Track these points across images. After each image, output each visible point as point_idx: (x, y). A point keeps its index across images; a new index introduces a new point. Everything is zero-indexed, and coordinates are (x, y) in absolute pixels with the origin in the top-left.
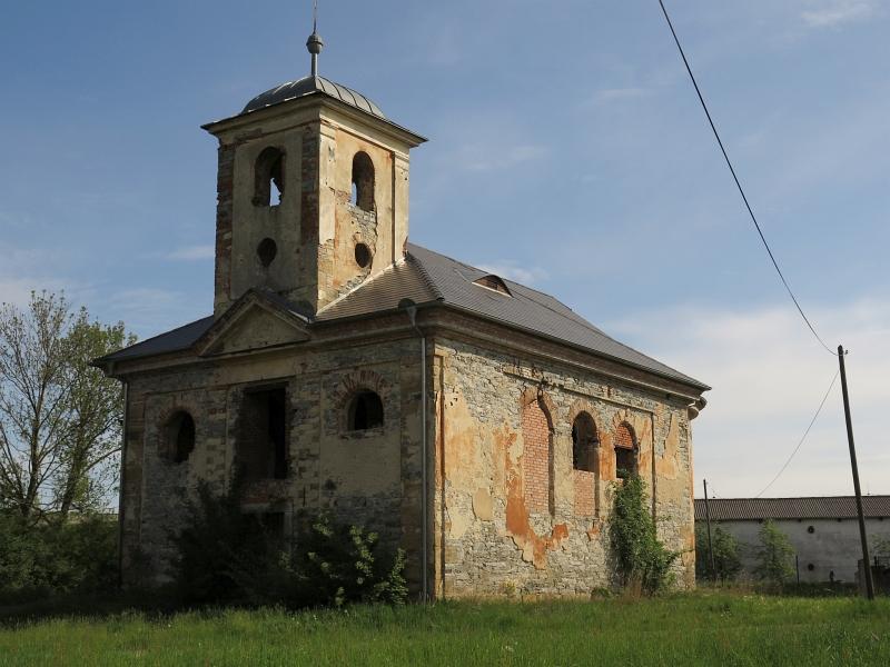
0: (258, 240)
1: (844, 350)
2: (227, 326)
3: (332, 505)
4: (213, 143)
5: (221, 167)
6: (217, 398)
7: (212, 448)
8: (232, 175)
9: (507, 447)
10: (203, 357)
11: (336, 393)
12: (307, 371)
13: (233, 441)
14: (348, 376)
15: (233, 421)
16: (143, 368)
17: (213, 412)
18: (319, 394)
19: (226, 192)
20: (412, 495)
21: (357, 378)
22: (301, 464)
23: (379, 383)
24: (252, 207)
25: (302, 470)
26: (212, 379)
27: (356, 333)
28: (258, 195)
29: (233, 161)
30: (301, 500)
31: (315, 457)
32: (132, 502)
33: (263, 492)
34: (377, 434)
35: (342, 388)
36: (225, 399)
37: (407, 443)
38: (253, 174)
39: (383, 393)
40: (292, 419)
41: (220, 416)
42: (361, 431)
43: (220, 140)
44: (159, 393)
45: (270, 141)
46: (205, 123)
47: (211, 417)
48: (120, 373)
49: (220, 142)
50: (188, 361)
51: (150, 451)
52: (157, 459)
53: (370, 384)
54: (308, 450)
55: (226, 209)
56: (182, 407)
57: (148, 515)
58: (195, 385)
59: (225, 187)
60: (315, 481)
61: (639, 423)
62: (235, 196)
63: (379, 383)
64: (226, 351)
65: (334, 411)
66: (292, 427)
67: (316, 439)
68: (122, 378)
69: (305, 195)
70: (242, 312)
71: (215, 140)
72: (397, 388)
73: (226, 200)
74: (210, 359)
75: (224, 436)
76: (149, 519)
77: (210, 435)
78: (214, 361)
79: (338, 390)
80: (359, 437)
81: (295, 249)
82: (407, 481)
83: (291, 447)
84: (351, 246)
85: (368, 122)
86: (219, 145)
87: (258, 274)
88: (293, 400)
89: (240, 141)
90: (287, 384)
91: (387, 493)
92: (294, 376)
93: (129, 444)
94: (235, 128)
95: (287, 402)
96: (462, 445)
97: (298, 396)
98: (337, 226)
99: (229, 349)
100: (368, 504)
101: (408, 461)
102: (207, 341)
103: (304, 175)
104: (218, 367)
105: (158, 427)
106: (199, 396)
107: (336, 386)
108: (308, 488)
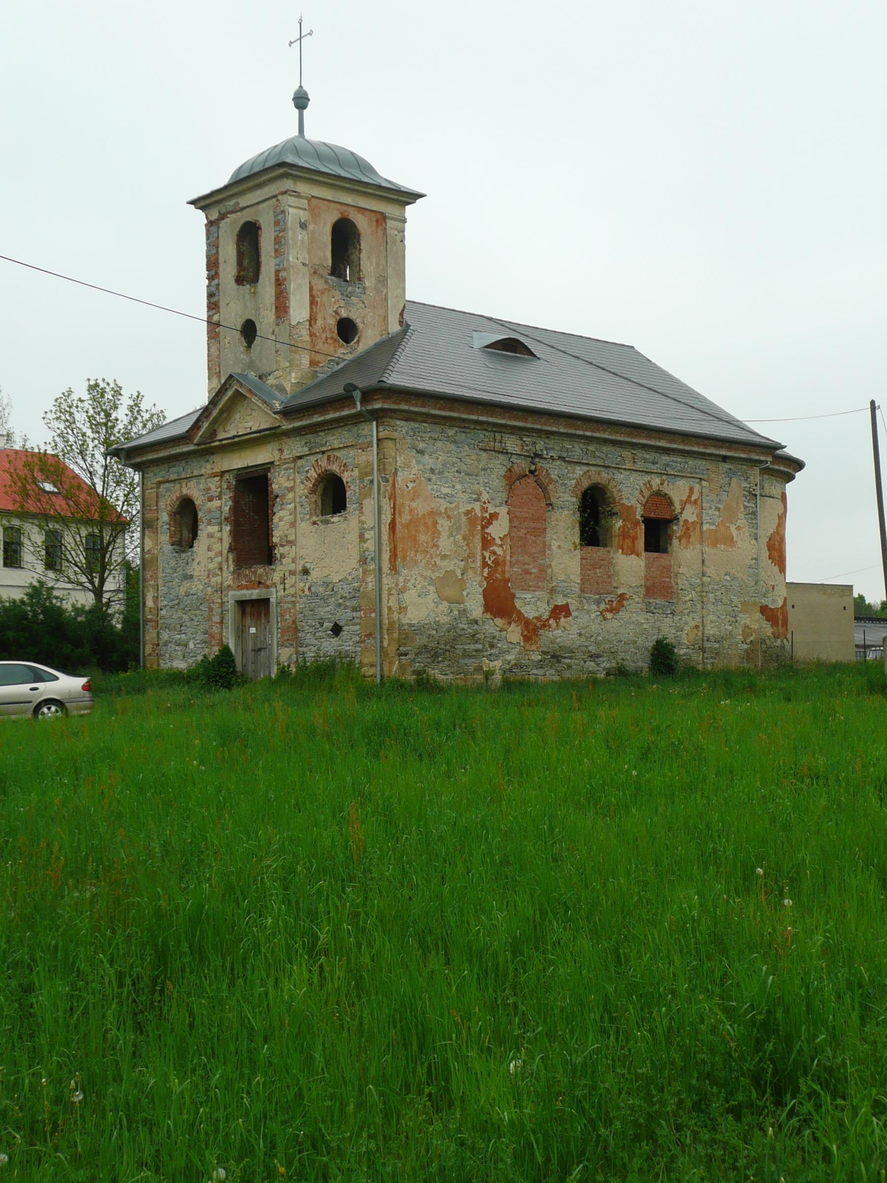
0: (239, 323)
1: (876, 405)
2: (215, 413)
3: (306, 589)
4: (200, 218)
5: (208, 245)
6: (213, 484)
7: (211, 536)
8: (217, 253)
9: (484, 527)
10: (198, 445)
11: (308, 479)
12: (283, 457)
13: (228, 528)
14: (317, 461)
15: (227, 508)
16: (150, 456)
17: (210, 499)
18: (294, 479)
19: (213, 272)
20: (369, 579)
21: (324, 463)
22: (282, 550)
23: (342, 468)
24: (235, 286)
25: (282, 556)
26: (209, 466)
27: (317, 418)
28: (242, 273)
29: (218, 237)
30: (282, 587)
31: (291, 543)
32: (151, 589)
33: (253, 578)
34: (341, 519)
35: (313, 474)
36: (220, 487)
37: (364, 528)
38: (235, 252)
39: (346, 477)
40: (274, 505)
41: (216, 503)
42: (328, 517)
43: (206, 215)
44: (168, 481)
45: (247, 216)
46: (194, 196)
47: (210, 504)
48: (133, 461)
49: (207, 218)
50: (185, 449)
51: (164, 538)
52: (170, 547)
53: (335, 468)
54: (286, 536)
55: (214, 289)
56: (186, 495)
57: (165, 603)
58: (196, 473)
59: (213, 265)
60: (292, 567)
61: (678, 491)
62: (221, 275)
63: (342, 468)
64: (219, 438)
65: (307, 497)
66: (274, 514)
67: (293, 525)
68: (137, 467)
69: (277, 272)
70: (226, 398)
71: (201, 215)
72: (356, 473)
73: (213, 279)
74: (203, 447)
75: (220, 524)
76: (165, 606)
77: (210, 523)
78: (206, 451)
79: (309, 475)
80: (327, 522)
81: (271, 330)
82: (365, 566)
83: (274, 533)
84: (332, 322)
85: (348, 185)
86: (206, 222)
87: (242, 356)
88: (273, 486)
89: (223, 217)
90: (269, 470)
91: (350, 578)
92: (272, 463)
93: (147, 532)
94: (218, 202)
95: (269, 488)
96: (422, 528)
97: (279, 482)
98: (313, 302)
99: (221, 435)
100: (335, 589)
101: (365, 546)
102: (199, 428)
103: (276, 251)
104: (213, 454)
105: (170, 516)
106: (200, 483)
107: (307, 472)
108: (287, 574)
